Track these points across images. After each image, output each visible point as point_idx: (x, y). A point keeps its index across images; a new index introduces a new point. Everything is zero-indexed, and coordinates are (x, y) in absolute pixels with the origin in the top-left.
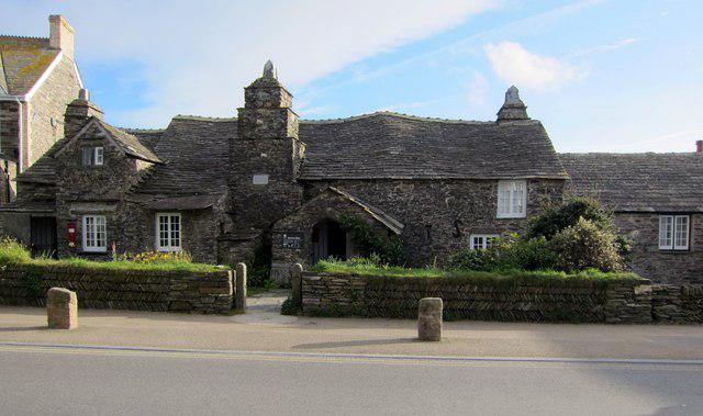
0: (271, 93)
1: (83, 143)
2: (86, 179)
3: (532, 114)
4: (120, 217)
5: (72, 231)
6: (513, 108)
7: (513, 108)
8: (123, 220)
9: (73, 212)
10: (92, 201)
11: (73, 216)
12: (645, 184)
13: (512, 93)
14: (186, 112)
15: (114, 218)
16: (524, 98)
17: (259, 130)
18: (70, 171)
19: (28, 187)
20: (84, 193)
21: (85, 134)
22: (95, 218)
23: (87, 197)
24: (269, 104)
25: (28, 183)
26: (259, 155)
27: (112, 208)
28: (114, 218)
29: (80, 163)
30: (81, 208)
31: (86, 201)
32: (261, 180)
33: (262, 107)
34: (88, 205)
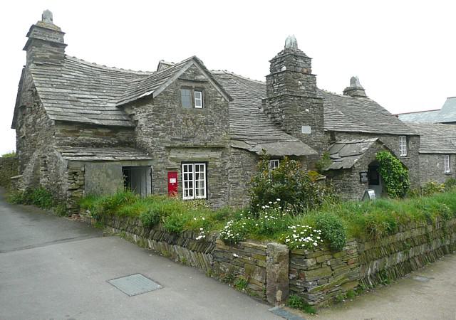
2: (190, 123)
4: (225, 163)
5: (173, 181)
7: (354, 91)
8: (229, 165)
9: (172, 159)
10: (196, 148)
11: (174, 163)
15: (218, 164)
16: (363, 83)
18: (171, 113)
19: (69, 128)
20: (187, 138)
22: (194, 166)
23: (191, 143)
26: (304, 110)
27: (217, 154)
29: (180, 106)
34: (190, 151)
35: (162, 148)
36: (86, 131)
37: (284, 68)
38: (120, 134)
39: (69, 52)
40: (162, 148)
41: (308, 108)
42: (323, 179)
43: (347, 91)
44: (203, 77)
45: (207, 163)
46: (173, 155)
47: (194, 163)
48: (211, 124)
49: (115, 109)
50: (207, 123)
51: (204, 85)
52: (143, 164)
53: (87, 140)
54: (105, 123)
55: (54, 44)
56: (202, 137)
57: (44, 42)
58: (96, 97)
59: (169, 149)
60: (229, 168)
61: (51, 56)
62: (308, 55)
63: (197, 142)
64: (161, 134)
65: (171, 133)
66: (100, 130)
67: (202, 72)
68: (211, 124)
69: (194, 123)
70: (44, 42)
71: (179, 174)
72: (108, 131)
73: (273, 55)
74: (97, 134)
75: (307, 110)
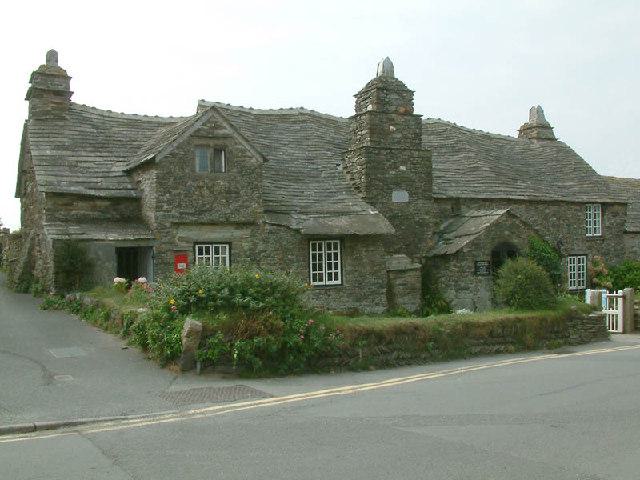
0: (403, 98)
1: (197, 141)
2: (206, 192)
3: (561, 134)
4: (255, 245)
6: (539, 129)
7: (539, 129)
8: (261, 247)
9: (181, 239)
10: (213, 223)
11: (184, 244)
12: (615, 199)
13: (538, 112)
14: (212, 98)
17: (394, 138)
20: (201, 212)
21: (199, 130)
22: (212, 248)
23: (205, 218)
24: (402, 110)
25: (61, 195)
27: (245, 232)
28: (246, 245)
30: (194, 233)
31: (203, 224)
32: (400, 196)
33: (396, 112)
35: (168, 225)
36: (80, 204)
37: (370, 108)
38: (122, 207)
39: (77, 99)
40: (168, 225)
41: (404, 163)
42: (416, 269)
43: (525, 130)
44: (228, 131)
45: (230, 244)
46: (182, 233)
47: (211, 243)
48: (236, 193)
49: (121, 174)
50: (229, 192)
51: (227, 142)
52: (142, 244)
53: (84, 215)
54: (102, 194)
55: (58, 93)
56: (221, 210)
57: (49, 89)
58: (101, 159)
59: (177, 225)
60: (262, 251)
61: (53, 109)
62: (410, 88)
63: (215, 216)
64: (165, 207)
65: (180, 206)
66: (99, 203)
67: (225, 124)
68: (236, 193)
69: (212, 192)
70: (49, 89)
71: (190, 258)
72: (107, 203)
73: (361, 86)
74: (94, 208)
75: (403, 168)
